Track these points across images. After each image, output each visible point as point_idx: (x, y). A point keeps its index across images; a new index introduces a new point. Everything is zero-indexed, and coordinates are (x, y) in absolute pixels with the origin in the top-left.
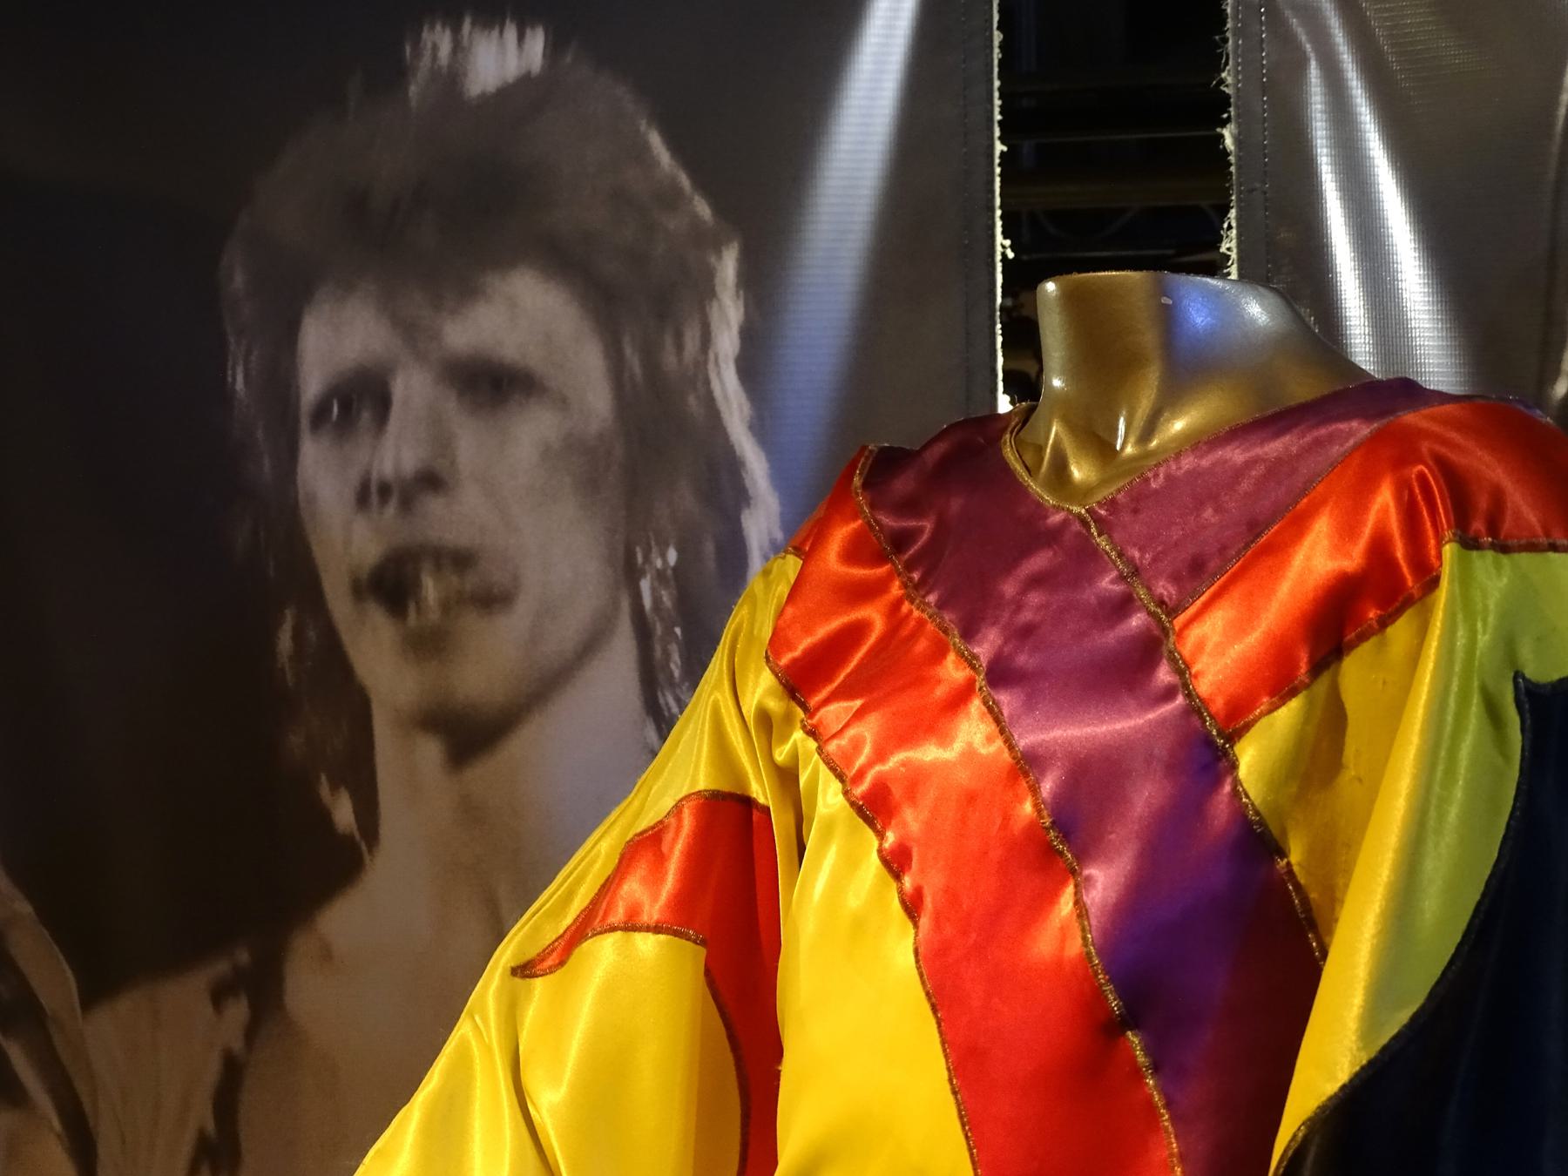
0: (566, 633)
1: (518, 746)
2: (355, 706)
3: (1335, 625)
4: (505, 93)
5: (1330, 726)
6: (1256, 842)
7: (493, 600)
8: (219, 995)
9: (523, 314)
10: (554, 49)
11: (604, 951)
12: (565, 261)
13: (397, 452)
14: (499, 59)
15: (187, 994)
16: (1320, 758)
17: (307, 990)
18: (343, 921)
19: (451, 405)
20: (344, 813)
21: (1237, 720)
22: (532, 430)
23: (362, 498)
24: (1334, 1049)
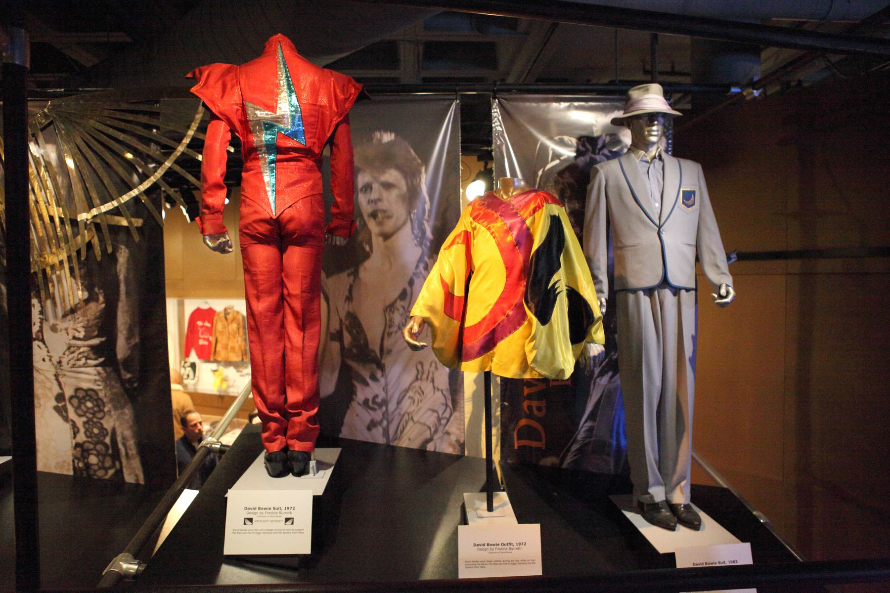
0: (400, 222)
1: (393, 238)
2: (370, 233)
3: (534, 211)
4: (389, 143)
5: (534, 219)
6: (528, 229)
7: (389, 217)
8: (349, 275)
9: (392, 175)
10: (396, 136)
11: (454, 247)
12: (399, 168)
13: (374, 196)
14: (388, 137)
15: (344, 276)
16: (533, 222)
17: (362, 274)
18: (367, 264)
19: (382, 189)
20: (367, 248)
21: (526, 218)
22: (394, 193)
23: (369, 202)
24: (535, 247)
